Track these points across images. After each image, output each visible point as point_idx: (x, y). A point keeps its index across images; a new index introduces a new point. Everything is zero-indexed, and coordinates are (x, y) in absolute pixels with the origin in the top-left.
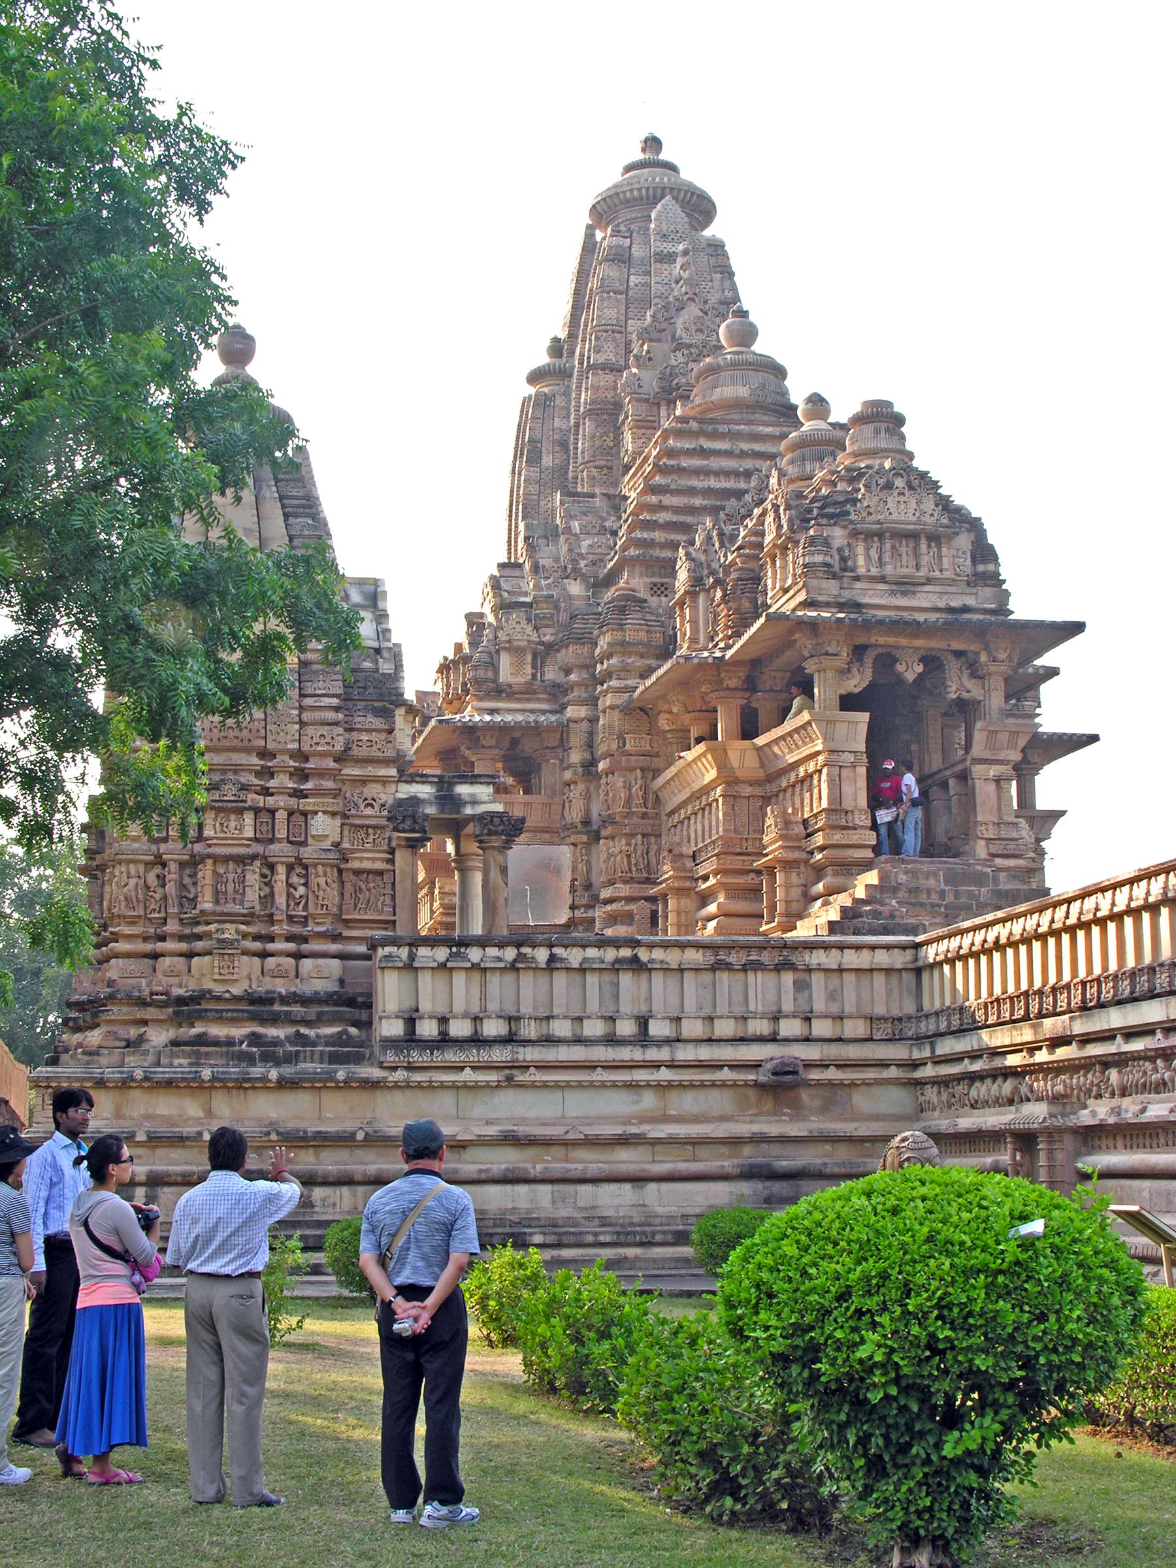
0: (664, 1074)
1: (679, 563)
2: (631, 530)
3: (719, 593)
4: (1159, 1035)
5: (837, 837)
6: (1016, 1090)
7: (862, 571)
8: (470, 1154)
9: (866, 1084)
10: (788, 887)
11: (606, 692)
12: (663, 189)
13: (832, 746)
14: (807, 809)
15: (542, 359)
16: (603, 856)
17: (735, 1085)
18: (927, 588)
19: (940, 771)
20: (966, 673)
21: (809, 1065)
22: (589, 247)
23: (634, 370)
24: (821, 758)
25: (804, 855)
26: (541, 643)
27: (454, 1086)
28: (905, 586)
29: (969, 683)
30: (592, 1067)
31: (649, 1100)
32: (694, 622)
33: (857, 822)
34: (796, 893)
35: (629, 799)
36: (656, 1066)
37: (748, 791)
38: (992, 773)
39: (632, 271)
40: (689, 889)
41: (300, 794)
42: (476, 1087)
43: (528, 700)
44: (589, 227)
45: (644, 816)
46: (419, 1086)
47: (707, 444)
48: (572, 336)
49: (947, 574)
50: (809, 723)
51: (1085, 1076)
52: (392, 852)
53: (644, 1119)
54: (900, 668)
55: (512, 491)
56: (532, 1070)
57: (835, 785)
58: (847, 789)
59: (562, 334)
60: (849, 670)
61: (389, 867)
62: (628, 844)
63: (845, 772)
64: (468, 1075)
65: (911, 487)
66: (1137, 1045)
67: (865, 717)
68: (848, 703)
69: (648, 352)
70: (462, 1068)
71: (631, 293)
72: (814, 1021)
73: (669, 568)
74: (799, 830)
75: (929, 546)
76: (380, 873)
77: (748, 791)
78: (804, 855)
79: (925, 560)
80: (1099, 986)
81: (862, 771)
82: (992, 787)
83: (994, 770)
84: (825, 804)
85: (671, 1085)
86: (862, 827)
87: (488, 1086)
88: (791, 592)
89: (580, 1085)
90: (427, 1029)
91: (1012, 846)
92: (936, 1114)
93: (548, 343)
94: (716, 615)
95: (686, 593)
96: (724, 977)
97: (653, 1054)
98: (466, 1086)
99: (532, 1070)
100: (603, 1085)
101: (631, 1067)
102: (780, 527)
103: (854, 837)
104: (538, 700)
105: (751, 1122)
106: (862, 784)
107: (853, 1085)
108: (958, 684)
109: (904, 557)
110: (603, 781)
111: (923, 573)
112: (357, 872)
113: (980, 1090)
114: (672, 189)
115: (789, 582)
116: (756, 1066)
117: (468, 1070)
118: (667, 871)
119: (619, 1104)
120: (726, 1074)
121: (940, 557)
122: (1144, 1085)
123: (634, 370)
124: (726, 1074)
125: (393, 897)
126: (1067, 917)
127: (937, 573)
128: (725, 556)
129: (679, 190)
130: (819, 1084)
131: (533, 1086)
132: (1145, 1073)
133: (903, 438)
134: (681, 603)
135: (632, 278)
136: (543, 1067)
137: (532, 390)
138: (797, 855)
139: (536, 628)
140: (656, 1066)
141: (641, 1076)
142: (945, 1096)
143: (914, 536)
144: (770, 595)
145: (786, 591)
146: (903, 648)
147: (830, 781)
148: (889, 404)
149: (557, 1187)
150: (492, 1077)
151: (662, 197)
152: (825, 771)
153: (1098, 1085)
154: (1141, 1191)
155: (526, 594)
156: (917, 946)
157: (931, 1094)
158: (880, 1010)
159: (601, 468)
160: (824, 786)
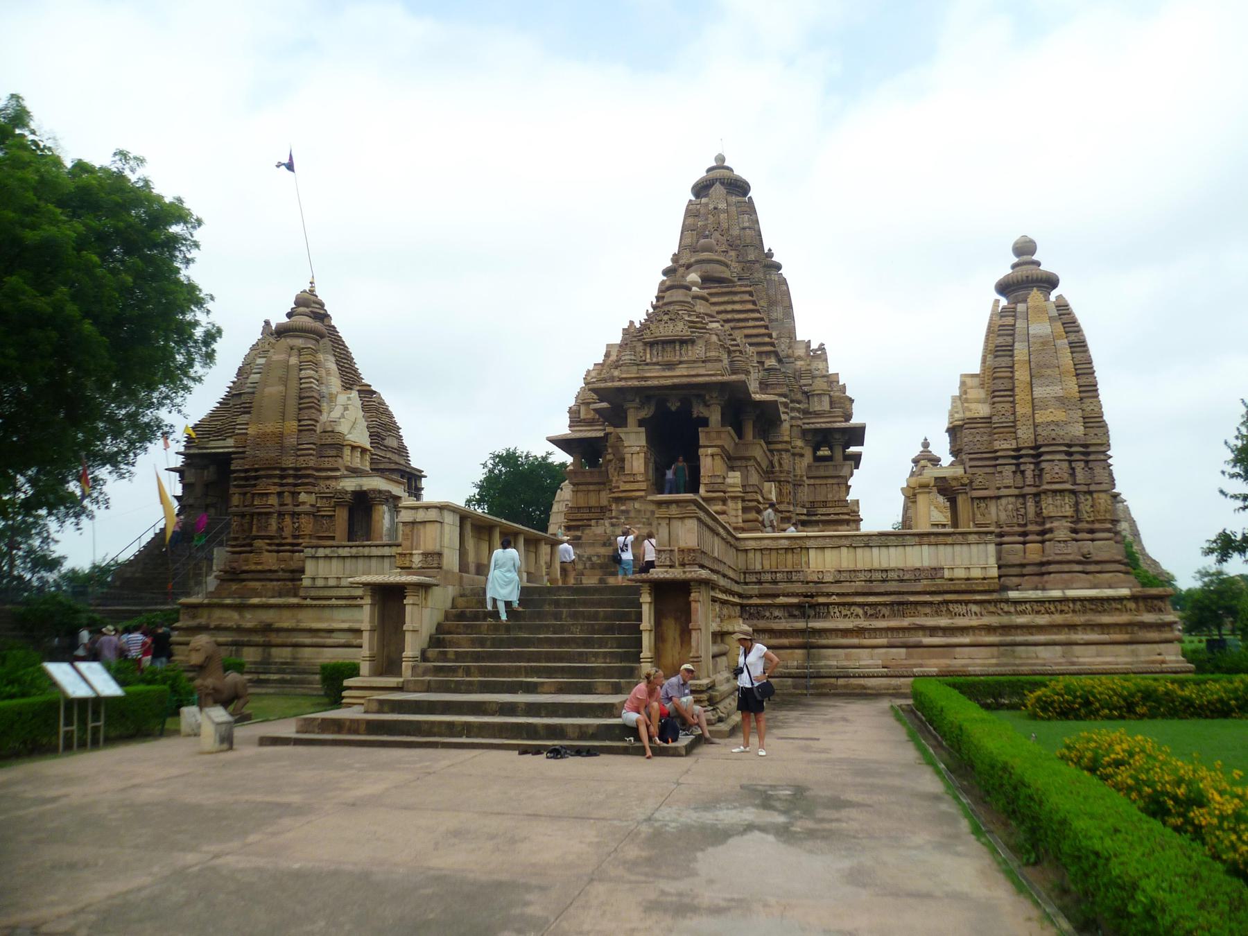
5: (628, 487)
8: (334, 635)
15: (669, 264)
28: (670, 366)
41: (296, 485)
42: (338, 606)
46: (315, 606)
58: (635, 464)
64: (334, 602)
67: (643, 429)
68: (641, 423)
76: (330, 516)
82: (709, 459)
83: (710, 451)
90: (320, 583)
103: (635, 486)
106: (642, 461)
108: (698, 410)
143: (672, 342)
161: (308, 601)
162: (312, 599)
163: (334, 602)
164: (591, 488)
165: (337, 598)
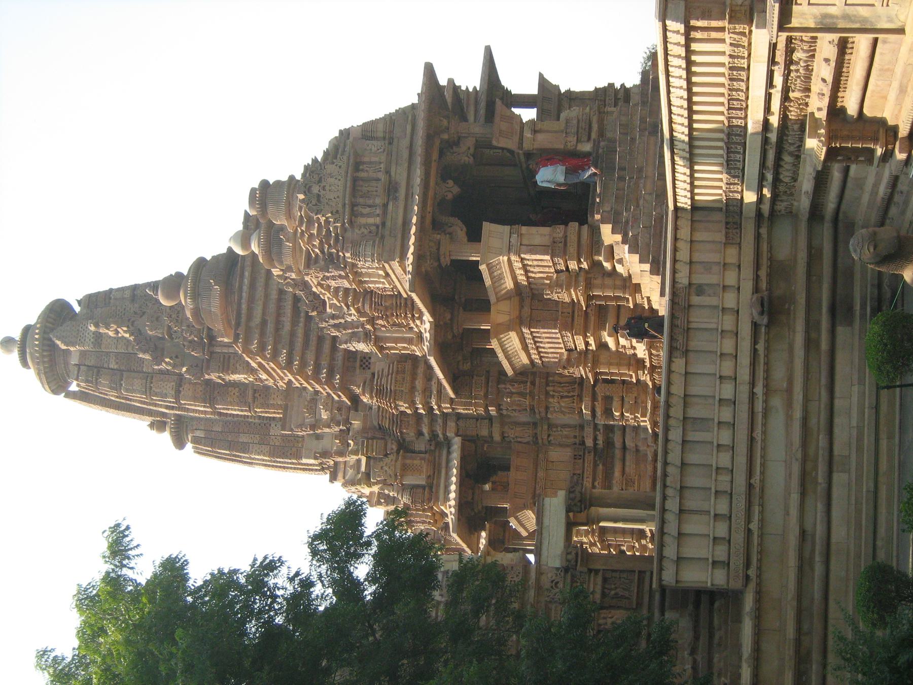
0: (759, 390)
1: (352, 348)
2: (319, 382)
3: (380, 322)
4: (776, 68)
6: (791, 154)
7: (378, 220)
9: (770, 249)
10: (603, 287)
11: (439, 407)
12: (44, 339)
13: (505, 249)
14: (547, 270)
15: (166, 437)
16: (561, 416)
17: (767, 341)
18: (393, 174)
19: (522, 172)
20: (455, 149)
21: (756, 289)
22: (82, 397)
23: (184, 369)
24: (513, 258)
25: (582, 273)
26: (398, 452)
27: (761, 536)
29: (463, 148)
30: (752, 440)
31: (777, 402)
32: (396, 340)
33: (561, 235)
34: (608, 281)
35: (521, 394)
36: (752, 396)
37: (526, 310)
38: (529, 135)
39: (106, 365)
40: (594, 356)
42: (762, 521)
43: (440, 464)
44: (66, 396)
45: (533, 383)
46: (760, 561)
47: (257, 320)
48: (150, 413)
49: (383, 158)
50: (488, 265)
51: (790, 111)
52: (590, 571)
53: (789, 405)
54: (450, 196)
55: (266, 465)
56: (752, 481)
57: (533, 249)
58: (537, 240)
59: (148, 420)
60: (450, 234)
61: (600, 574)
62: (553, 396)
63: (525, 242)
64: (754, 526)
65: (320, 181)
66: (778, 80)
68: (475, 236)
69: (171, 358)
70: (749, 530)
71: (123, 368)
72: (727, 283)
73: (351, 356)
74: (563, 276)
75: (362, 170)
76: (605, 580)
77: (526, 310)
78: (582, 273)
79: (372, 175)
80: (733, 99)
81: (524, 229)
82: (540, 137)
84: (548, 257)
85: (766, 386)
86: (565, 232)
87: (761, 512)
88: (390, 272)
89: (763, 449)
91: (582, 124)
92: (796, 204)
93: (154, 432)
94: (394, 325)
95: (375, 344)
96: (694, 344)
97: (744, 396)
98: (761, 528)
99: (752, 481)
100: (764, 433)
101: (753, 412)
102: (340, 277)
104: (440, 457)
105: (794, 332)
106: (534, 230)
107: (770, 259)
109: (371, 189)
110: (505, 412)
111: (382, 176)
112: (604, 595)
113: (785, 176)
114: (45, 332)
115: (381, 272)
116: (755, 326)
117: (752, 526)
118: (581, 371)
119: (777, 422)
120: (761, 347)
121: (371, 163)
122: (805, 77)
123: (184, 369)
124: (761, 347)
125: (621, 571)
126: (682, 116)
127: (382, 166)
128: (350, 315)
129: (46, 327)
130: (769, 283)
131: (762, 481)
132: (799, 77)
133: (278, 183)
134: (381, 349)
135: (111, 366)
136: (750, 473)
137: (189, 446)
138: (581, 279)
139: (386, 455)
140: (752, 396)
141: (759, 406)
142: (784, 198)
143: (355, 180)
144: (387, 286)
145: (387, 275)
146: (435, 194)
147: (532, 252)
148: (253, 191)
149: (835, 468)
150: (756, 509)
151: (50, 340)
152: (522, 256)
153: (799, 105)
154: (877, 85)
155: (359, 461)
156: (676, 208)
157: (781, 206)
158: (720, 237)
159: (254, 397)
160: (534, 257)
161: (752, 572)
162: (748, 565)
163: (754, 526)
164: (541, 474)
165: (749, 520)
